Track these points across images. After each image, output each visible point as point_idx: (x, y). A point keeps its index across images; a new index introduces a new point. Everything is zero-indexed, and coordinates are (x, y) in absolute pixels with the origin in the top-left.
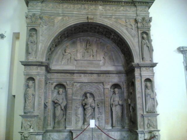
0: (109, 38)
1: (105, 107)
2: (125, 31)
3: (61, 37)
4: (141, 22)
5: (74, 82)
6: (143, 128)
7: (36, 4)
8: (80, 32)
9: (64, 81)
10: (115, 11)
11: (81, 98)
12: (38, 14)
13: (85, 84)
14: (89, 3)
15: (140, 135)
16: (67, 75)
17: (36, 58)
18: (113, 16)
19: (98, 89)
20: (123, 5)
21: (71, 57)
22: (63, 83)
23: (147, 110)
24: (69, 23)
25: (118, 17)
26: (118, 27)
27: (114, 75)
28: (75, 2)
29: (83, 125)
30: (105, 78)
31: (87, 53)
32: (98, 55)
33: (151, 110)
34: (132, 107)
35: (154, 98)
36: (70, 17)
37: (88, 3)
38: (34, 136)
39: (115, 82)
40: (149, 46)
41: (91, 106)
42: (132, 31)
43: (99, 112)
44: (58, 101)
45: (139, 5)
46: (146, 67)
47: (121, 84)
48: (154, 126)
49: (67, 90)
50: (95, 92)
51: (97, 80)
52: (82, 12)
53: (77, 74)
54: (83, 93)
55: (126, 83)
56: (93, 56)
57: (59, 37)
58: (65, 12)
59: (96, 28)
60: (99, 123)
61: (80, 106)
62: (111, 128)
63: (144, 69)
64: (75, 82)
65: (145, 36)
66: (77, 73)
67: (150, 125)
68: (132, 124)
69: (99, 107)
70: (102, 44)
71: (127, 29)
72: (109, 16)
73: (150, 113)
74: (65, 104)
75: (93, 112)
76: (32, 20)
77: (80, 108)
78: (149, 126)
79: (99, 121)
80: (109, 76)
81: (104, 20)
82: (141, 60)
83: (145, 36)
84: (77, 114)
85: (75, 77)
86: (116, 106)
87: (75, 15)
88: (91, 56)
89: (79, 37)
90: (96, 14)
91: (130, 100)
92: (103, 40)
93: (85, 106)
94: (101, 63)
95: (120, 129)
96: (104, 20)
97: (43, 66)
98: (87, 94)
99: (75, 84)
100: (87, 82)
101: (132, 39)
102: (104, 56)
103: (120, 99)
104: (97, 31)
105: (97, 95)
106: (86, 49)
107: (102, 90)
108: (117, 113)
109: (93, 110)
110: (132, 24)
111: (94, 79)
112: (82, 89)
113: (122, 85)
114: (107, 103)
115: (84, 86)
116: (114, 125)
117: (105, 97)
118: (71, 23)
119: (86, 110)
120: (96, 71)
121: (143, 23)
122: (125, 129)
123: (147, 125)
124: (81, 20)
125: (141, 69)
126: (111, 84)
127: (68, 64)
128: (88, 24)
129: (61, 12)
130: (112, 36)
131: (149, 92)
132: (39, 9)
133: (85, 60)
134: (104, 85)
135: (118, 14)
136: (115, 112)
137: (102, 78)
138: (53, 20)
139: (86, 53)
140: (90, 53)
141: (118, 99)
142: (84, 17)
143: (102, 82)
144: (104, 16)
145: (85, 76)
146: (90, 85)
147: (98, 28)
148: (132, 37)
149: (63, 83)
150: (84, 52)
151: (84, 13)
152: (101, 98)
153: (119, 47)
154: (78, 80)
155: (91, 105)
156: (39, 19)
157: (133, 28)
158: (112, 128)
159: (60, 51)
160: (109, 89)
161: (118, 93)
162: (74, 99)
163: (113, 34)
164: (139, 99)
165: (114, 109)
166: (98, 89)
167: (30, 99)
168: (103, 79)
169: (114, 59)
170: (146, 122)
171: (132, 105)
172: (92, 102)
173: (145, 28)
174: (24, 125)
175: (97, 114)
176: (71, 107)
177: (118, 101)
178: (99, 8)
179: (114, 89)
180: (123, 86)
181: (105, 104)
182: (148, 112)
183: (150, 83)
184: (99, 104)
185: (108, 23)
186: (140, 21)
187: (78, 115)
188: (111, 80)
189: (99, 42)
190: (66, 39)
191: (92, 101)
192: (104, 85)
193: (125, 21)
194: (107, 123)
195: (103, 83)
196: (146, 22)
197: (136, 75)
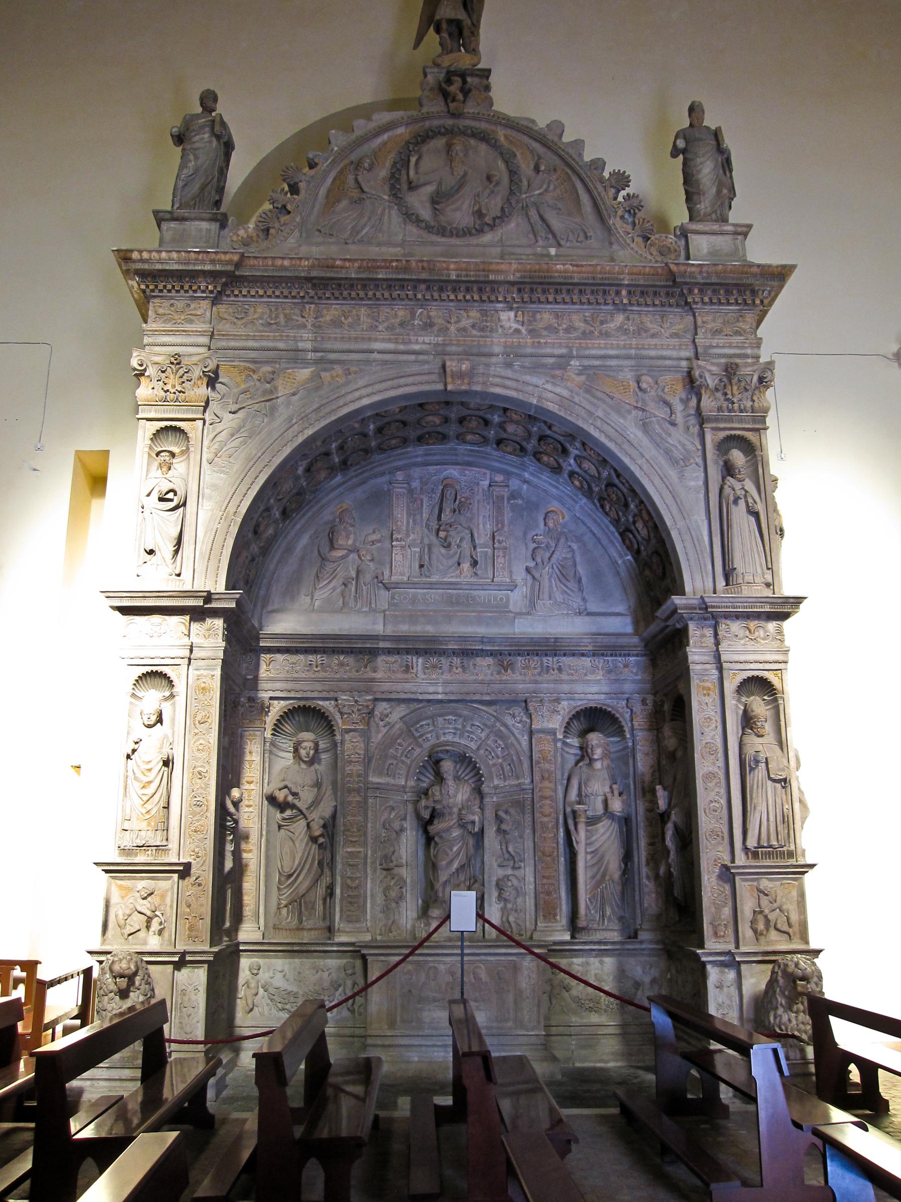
0: (557, 470)
1: (538, 826)
2: (635, 433)
3: (308, 470)
4: (717, 390)
5: (376, 700)
6: (732, 939)
7: (189, 305)
8: (405, 441)
9: (324, 695)
10: (584, 333)
11: (411, 783)
12: (195, 359)
13: (431, 710)
14: (452, 297)
15: (713, 974)
16: (341, 664)
17: (179, 575)
18: (570, 357)
19: (500, 735)
20: (625, 301)
21: (358, 572)
22: (320, 703)
23: (752, 843)
24: (350, 397)
25: (597, 363)
26: (600, 413)
27: (586, 661)
28: (378, 294)
29: (419, 918)
30: (539, 678)
31: (443, 551)
32: (500, 561)
33: (774, 843)
34: (676, 827)
35: (785, 780)
36: (353, 369)
37: (444, 296)
38: (171, 967)
39: (590, 696)
40: (760, 507)
41: (462, 825)
42: (670, 435)
43: (507, 856)
44: (295, 794)
45: (706, 299)
46: (748, 616)
47: (619, 708)
48: (790, 925)
49: (338, 738)
52: (417, 342)
53: (391, 659)
54: (420, 754)
55: (644, 702)
56: (475, 563)
57: (300, 470)
58: (328, 346)
59: (487, 423)
60: (503, 910)
61: (407, 825)
62: (567, 937)
63: (736, 627)
64: (378, 696)
65: (738, 457)
66: (389, 652)
67: (767, 921)
68: (677, 919)
69: (504, 827)
70: (520, 502)
71: (645, 427)
72: (551, 360)
73: (768, 855)
74: (328, 813)
75: (472, 851)
76: (168, 387)
78: (761, 926)
79: (506, 900)
80: (560, 669)
81: (528, 378)
82: (721, 583)
83: (738, 457)
85: (379, 675)
86: (592, 821)
87: (376, 356)
88: (466, 566)
89: (399, 469)
90: (486, 350)
91: (666, 793)
92: (525, 481)
93: (430, 821)
94: (517, 599)
95: (613, 943)
96: (528, 378)
97: (215, 613)
98: (442, 763)
99: (382, 707)
100: (440, 697)
101: (673, 474)
102: (532, 564)
103: (615, 786)
104: (492, 434)
105: (494, 765)
106: (438, 530)
108: (601, 859)
109: (471, 841)
110: (668, 398)
111: (476, 682)
112: (417, 735)
113: (627, 716)
114: (547, 810)
116: (582, 923)
117: (537, 777)
118: (360, 398)
120: (491, 640)
121: (726, 394)
122: (641, 942)
123: (753, 922)
124: (410, 380)
125: (722, 628)
126: (566, 708)
127: (345, 604)
128: (447, 403)
129: (309, 345)
130: (572, 461)
131: (760, 748)
132: (202, 334)
133: (431, 586)
134: (530, 716)
135: (597, 347)
136: (587, 853)
137: (517, 676)
138: (268, 386)
139: (440, 551)
140: (459, 546)
141: (607, 789)
142: (426, 367)
143: (522, 697)
144: (527, 362)
145: (434, 667)
146: (460, 716)
147: (496, 419)
148: (674, 462)
150: (426, 541)
151: (424, 347)
153: (607, 514)
154: (399, 687)
156: (199, 382)
157: (679, 418)
158: (573, 937)
159: (305, 540)
161: (605, 756)
162: (378, 787)
163: (576, 452)
164: (711, 785)
165: (581, 836)
166: (500, 735)
167: (150, 782)
168: (524, 682)
169: (584, 580)
170: (747, 907)
171: (675, 817)
172: (468, 800)
173: (741, 421)
174: (116, 916)
175: (495, 865)
176: (362, 830)
177: (600, 799)
178: (499, 320)
179: (583, 734)
180: (632, 720)
181: (537, 815)
182: (755, 855)
183: (768, 703)
184: (506, 812)
185: (550, 395)
186: (711, 382)
188: (566, 687)
189: (506, 493)
190: (339, 478)
191: (465, 797)
193: (633, 384)
194: (545, 909)
195: (526, 701)
196: (746, 390)
197: (691, 658)
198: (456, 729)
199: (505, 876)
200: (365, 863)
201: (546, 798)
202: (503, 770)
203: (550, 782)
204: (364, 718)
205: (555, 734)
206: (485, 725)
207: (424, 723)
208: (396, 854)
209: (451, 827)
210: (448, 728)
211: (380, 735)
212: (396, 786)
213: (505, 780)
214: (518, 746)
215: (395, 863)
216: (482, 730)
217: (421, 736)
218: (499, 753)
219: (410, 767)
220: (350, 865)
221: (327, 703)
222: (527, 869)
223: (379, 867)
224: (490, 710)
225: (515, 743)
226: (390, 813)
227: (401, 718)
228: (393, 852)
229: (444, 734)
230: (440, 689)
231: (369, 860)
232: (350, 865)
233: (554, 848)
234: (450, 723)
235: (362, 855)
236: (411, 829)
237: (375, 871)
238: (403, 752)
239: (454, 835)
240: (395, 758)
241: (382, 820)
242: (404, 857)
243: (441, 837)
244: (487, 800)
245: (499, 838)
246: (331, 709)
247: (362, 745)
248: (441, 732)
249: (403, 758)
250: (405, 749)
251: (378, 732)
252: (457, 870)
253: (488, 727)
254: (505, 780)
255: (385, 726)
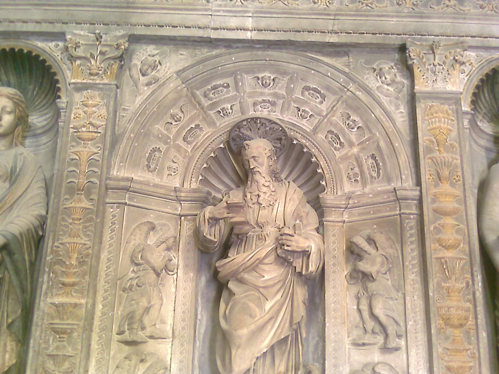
1: (433, 268)
5: (135, 39)
9: (45, 28)
22: (40, 44)
43: (370, 324)
49: (62, 102)
50: (321, 136)
51: (348, 23)
64: (140, 31)
69: (363, 266)
75: (301, 311)
77: (170, 281)
84: (141, 335)
100: (248, 35)
105: (345, 158)
107: (391, 108)
109: (301, 293)
112: (206, 103)
114: (450, 236)
115: (233, 74)
119: (231, 294)
134: (409, 71)
143: (396, 41)
149: (40, 44)
152: (390, 187)
155: (280, 244)
160: (466, 107)
175: (347, 341)
181: (430, 245)
184: (371, 240)
187: (151, 346)
191: (291, 207)
192: (409, 71)
198: (276, 95)
199: (366, 365)
200: (88, 328)
201: (446, 214)
202: (360, 166)
203: (452, 185)
204: (110, 65)
205: (458, 102)
206: (328, 88)
207: (220, 82)
208: (154, 312)
209: (261, 261)
210: (262, 94)
211: (139, 100)
212: (162, 187)
213: (364, 184)
214: (388, 124)
215: (148, 331)
216: (324, 97)
217: (214, 105)
218: (353, 138)
219: (191, 159)
220: (56, 331)
221: (52, 45)
222: (413, 352)
223: (116, 337)
224: (338, 62)
225: (383, 118)
226: (148, 234)
227: (179, 73)
228: (147, 310)
229: (255, 104)
230: (249, 23)
231: (96, 322)
232: (56, 331)
233: (468, 310)
234: (265, 85)
235: (82, 312)
236: (186, 266)
237: (107, 345)
238: (178, 133)
239: (267, 277)
240: (165, 140)
241: (131, 246)
242: (170, 321)
243: (241, 281)
244: (331, 217)
245: (354, 289)
246: (58, 55)
247: (103, 111)
248: (250, 101)
249: (180, 142)
250: (183, 128)
251: (136, 93)
252: (272, 348)
253: (335, 93)
254: (364, 184)
255: (148, 84)
